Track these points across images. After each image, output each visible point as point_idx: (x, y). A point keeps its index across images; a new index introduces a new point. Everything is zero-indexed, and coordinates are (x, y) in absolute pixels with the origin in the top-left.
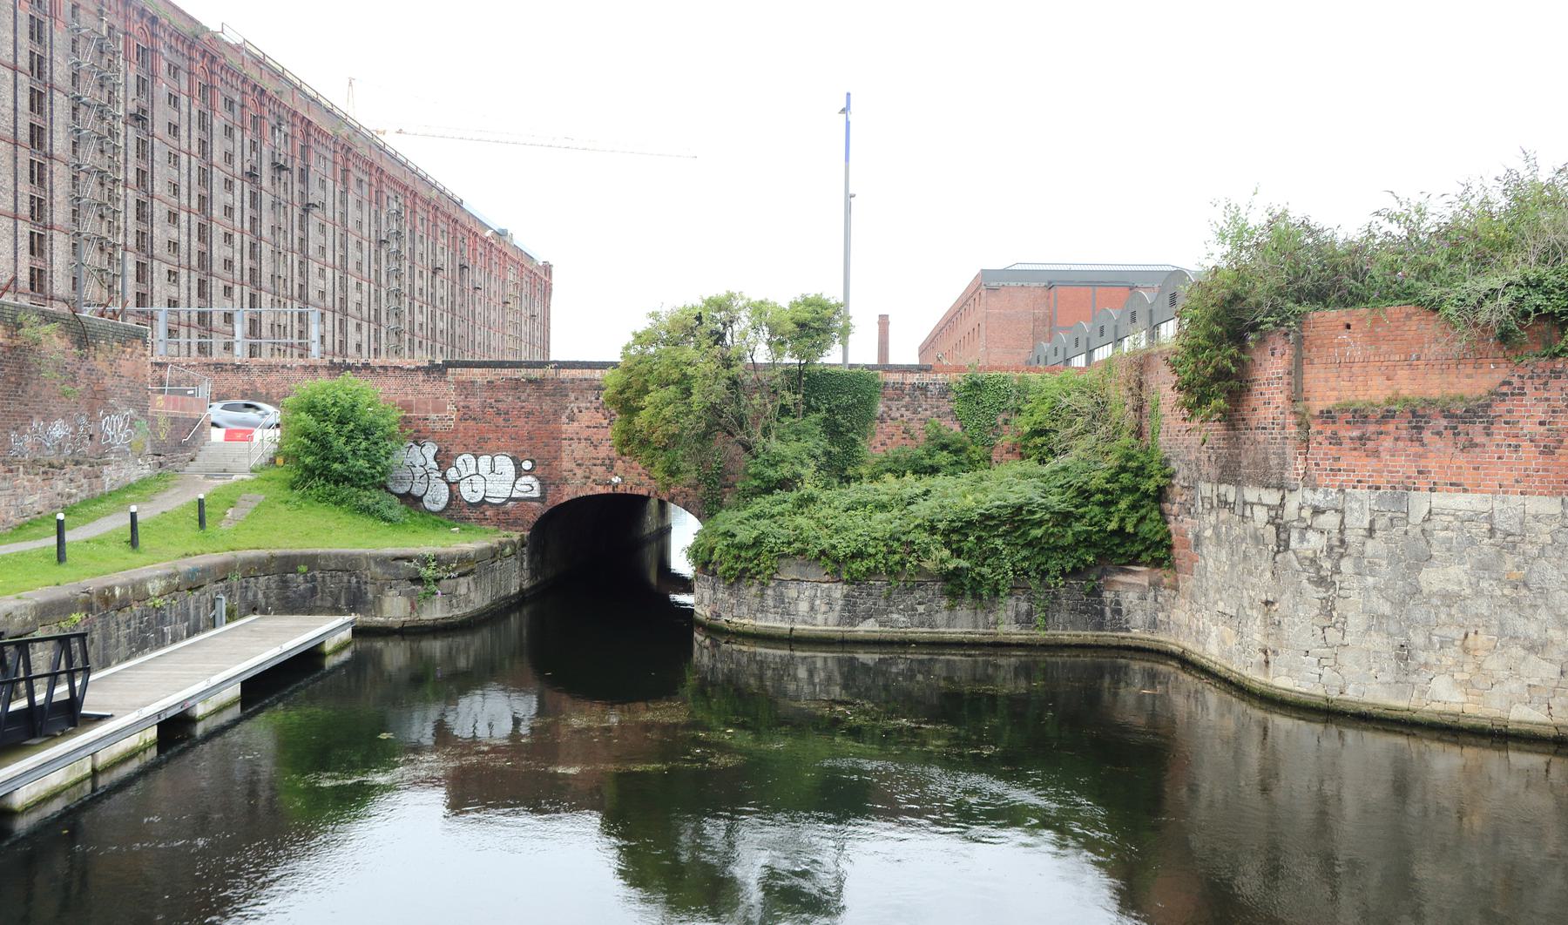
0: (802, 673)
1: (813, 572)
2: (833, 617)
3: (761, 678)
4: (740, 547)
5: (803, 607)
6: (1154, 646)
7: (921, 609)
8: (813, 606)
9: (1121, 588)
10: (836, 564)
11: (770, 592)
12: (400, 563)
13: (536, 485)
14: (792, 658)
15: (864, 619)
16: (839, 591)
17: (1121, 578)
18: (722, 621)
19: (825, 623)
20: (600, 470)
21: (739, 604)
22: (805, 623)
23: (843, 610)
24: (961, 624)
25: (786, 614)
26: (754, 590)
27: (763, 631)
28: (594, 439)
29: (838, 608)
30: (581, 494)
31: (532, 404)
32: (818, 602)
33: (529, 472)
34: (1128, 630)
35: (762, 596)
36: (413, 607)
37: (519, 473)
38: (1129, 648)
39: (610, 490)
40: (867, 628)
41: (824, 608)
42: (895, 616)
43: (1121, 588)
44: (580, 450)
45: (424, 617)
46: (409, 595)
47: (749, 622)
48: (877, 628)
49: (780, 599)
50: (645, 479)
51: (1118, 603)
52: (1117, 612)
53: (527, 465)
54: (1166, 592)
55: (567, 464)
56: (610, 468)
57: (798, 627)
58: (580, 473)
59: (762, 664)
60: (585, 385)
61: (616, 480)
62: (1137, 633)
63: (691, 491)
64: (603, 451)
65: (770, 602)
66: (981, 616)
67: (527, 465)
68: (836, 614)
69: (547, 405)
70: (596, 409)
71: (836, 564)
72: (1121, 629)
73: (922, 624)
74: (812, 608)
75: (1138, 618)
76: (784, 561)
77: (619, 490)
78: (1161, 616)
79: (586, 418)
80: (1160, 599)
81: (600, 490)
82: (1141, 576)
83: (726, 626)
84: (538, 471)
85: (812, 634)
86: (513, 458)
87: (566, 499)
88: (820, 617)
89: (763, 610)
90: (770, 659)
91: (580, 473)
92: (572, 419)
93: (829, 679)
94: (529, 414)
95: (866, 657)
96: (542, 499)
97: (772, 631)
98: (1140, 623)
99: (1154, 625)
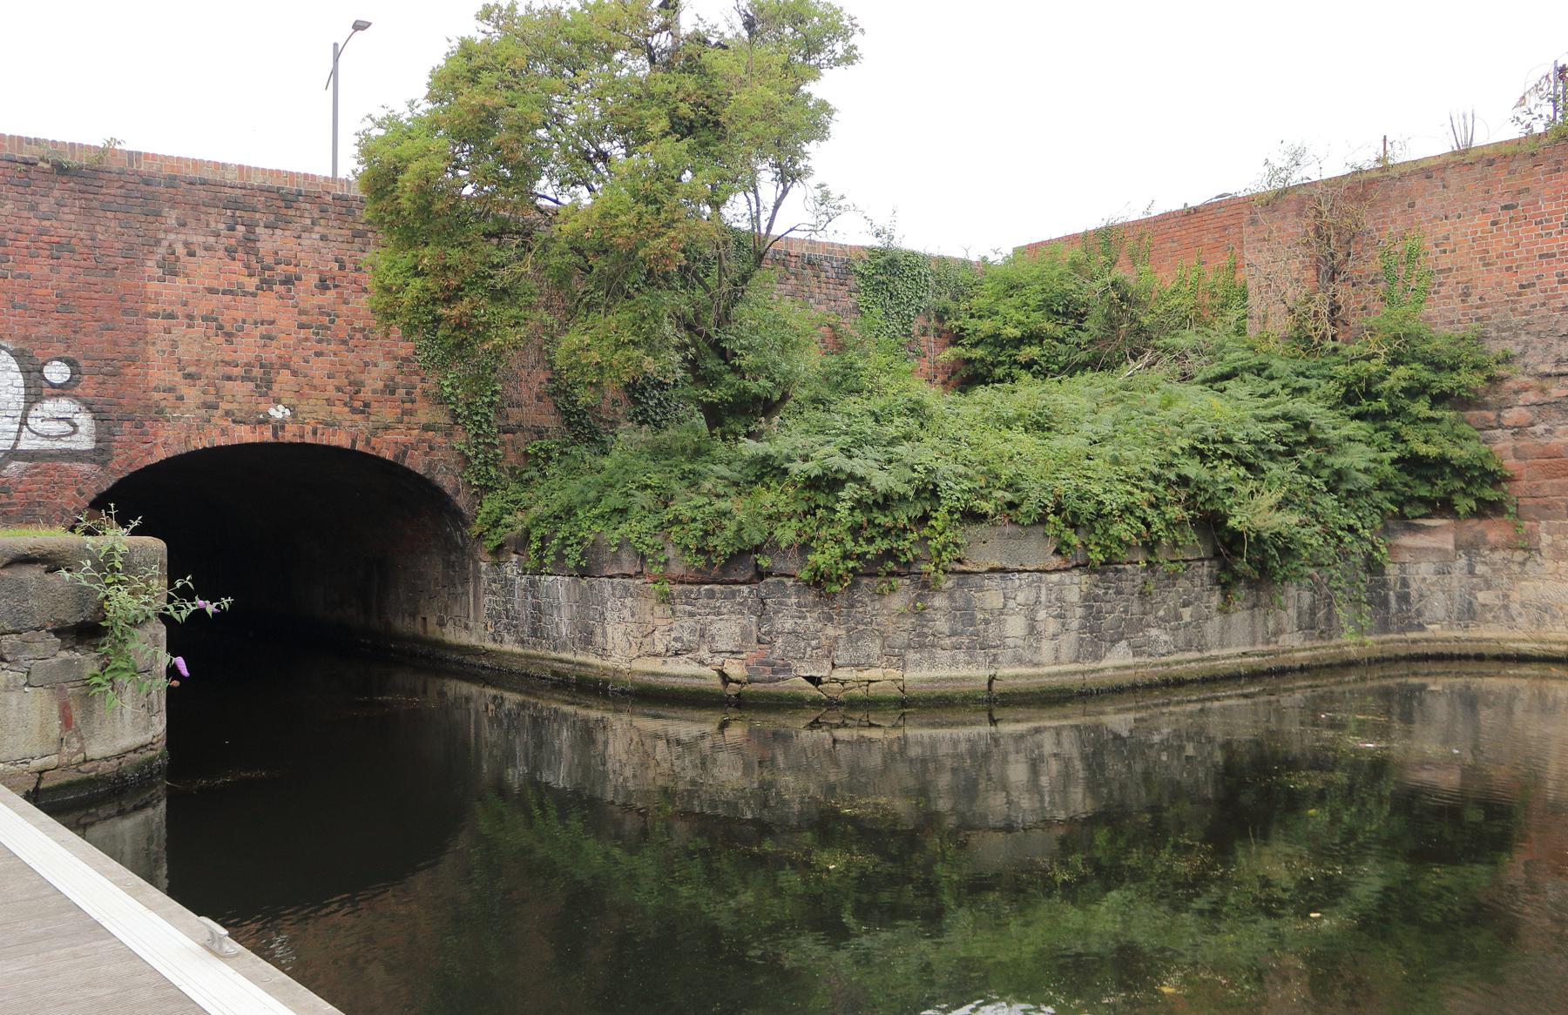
0: (1018, 772)
1: (1037, 552)
2: (1069, 642)
3: (923, 791)
4: (886, 502)
5: (1015, 626)
6: (1470, 649)
7: (1187, 613)
8: (1029, 623)
9: (1407, 557)
10: (1076, 529)
11: (939, 601)
12: (32, 574)
13: (84, 420)
14: (996, 740)
15: (1114, 642)
16: (1075, 586)
17: (1407, 540)
18: (796, 683)
19: (1054, 661)
20: (240, 390)
21: (854, 638)
22: (1020, 661)
23: (1083, 627)
24: (1234, 638)
25: (981, 646)
26: (897, 602)
27: (926, 690)
28: (226, 318)
29: (1075, 624)
30: (198, 444)
31: (69, 224)
32: (1042, 615)
33: (60, 390)
34: (1421, 627)
35: (920, 614)
36: (67, 721)
37: (36, 390)
38: (1426, 658)
39: (267, 436)
40: (1118, 661)
41: (1052, 626)
42: (1154, 632)
43: (1407, 557)
44: (192, 342)
45: (96, 750)
46: (52, 684)
47: (882, 676)
48: (1130, 661)
49: (965, 614)
50: (341, 412)
51: (1405, 583)
52: (1404, 598)
53: (57, 373)
54: (1497, 556)
55: (160, 373)
56: (265, 386)
57: (1006, 671)
58: (192, 395)
59: (927, 763)
60: (202, 194)
61: (278, 412)
62: (1439, 632)
63: (439, 439)
64: (247, 349)
65: (942, 625)
66: (1259, 620)
67: (57, 373)
68: (1073, 636)
69: (108, 230)
70: (231, 252)
71: (1076, 529)
72: (1411, 627)
73: (1188, 646)
74: (1032, 629)
75: (1438, 605)
76: (977, 530)
77: (288, 436)
78: (1483, 597)
79: (205, 270)
80: (1480, 569)
81: (245, 435)
82: (1440, 535)
83: (811, 691)
84: (88, 388)
85: (1033, 685)
86: (18, 355)
87: (160, 455)
88: (1047, 646)
89: (923, 643)
90: (944, 749)
91: (192, 395)
92: (170, 269)
93: (1066, 776)
94: (60, 249)
95: (1118, 720)
96: (100, 454)
97: (949, 689)
98: (1441, 613)
99: (1469, 613)
